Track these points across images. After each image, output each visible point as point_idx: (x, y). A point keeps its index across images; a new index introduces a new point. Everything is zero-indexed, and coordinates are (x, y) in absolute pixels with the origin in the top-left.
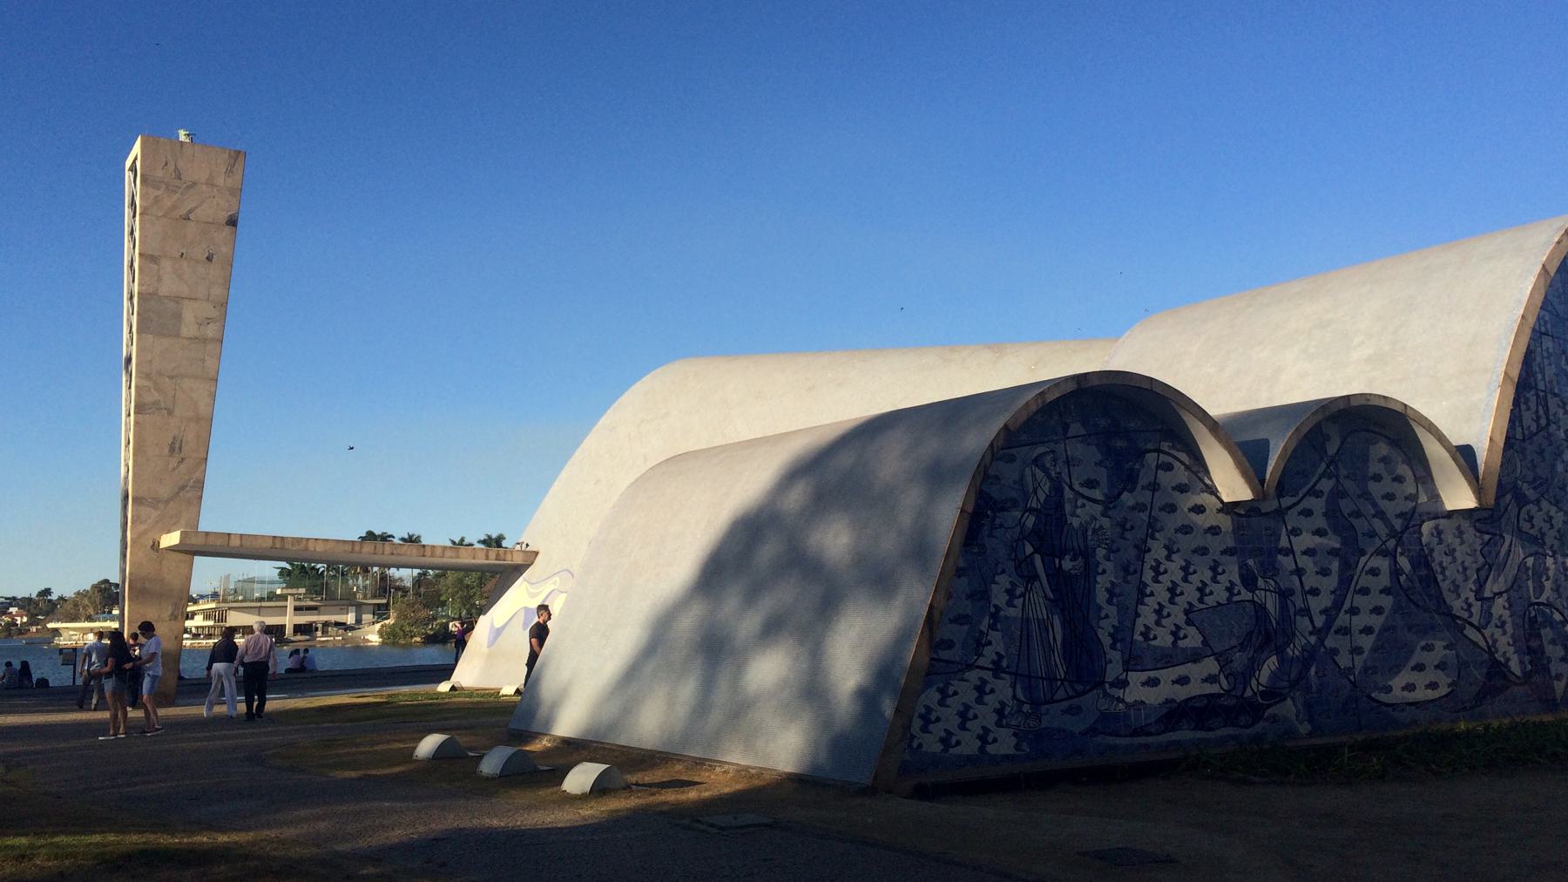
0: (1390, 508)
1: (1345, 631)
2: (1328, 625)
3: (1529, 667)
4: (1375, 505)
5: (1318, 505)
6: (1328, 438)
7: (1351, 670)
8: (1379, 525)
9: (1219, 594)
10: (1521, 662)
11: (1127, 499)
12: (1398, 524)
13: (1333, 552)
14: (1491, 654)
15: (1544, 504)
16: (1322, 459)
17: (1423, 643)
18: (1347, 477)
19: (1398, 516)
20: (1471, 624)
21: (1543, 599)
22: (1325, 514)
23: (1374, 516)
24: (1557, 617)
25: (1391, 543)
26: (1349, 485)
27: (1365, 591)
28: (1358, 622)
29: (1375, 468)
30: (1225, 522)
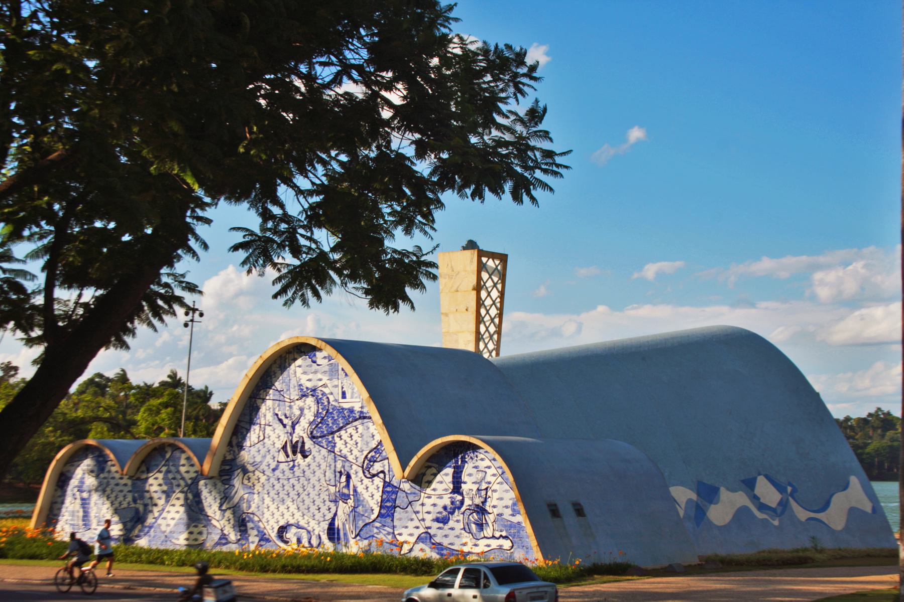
0: (187, 476)
1: (164, 518)
2: (160, 515)
3: (239, 537)
4: (181, 475)
5: (160, 476)
6: (166, 452)
7: (164, 532)
8: (182, 483)
9: (125, 505)
10: (236, 535)
11: (102, 476)
12: (189, 482)
13: (164, 492)
14: (222, 530)
15: (257, 473)
16: (163, 460)
17: (193, 524)
18: (172, 465)
19: (190, 479)
20: (215, 519)
21: (250, 511)
22: (163, 479)
23: (181, 479)
24: (256, 519)
25: (186, 489)
26: (172, 468)
27: (173, 505)
28: (169, 516)
29: (183, 462)
30: (129, 482)
